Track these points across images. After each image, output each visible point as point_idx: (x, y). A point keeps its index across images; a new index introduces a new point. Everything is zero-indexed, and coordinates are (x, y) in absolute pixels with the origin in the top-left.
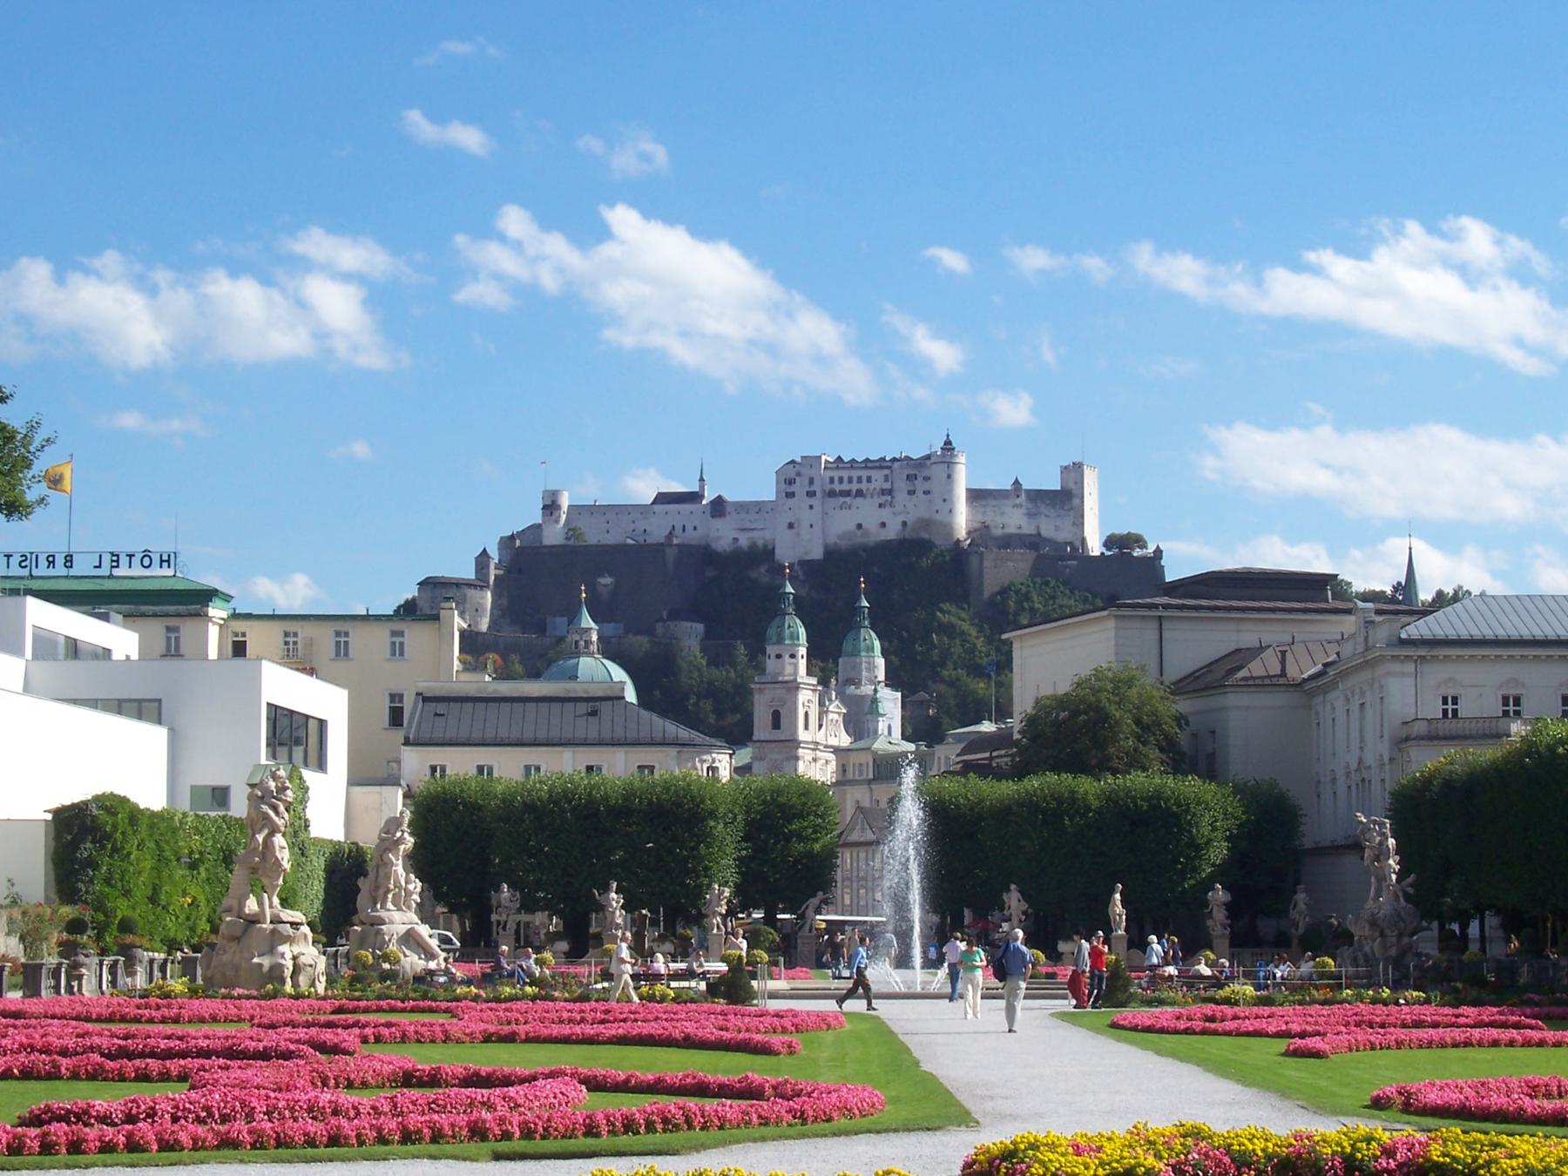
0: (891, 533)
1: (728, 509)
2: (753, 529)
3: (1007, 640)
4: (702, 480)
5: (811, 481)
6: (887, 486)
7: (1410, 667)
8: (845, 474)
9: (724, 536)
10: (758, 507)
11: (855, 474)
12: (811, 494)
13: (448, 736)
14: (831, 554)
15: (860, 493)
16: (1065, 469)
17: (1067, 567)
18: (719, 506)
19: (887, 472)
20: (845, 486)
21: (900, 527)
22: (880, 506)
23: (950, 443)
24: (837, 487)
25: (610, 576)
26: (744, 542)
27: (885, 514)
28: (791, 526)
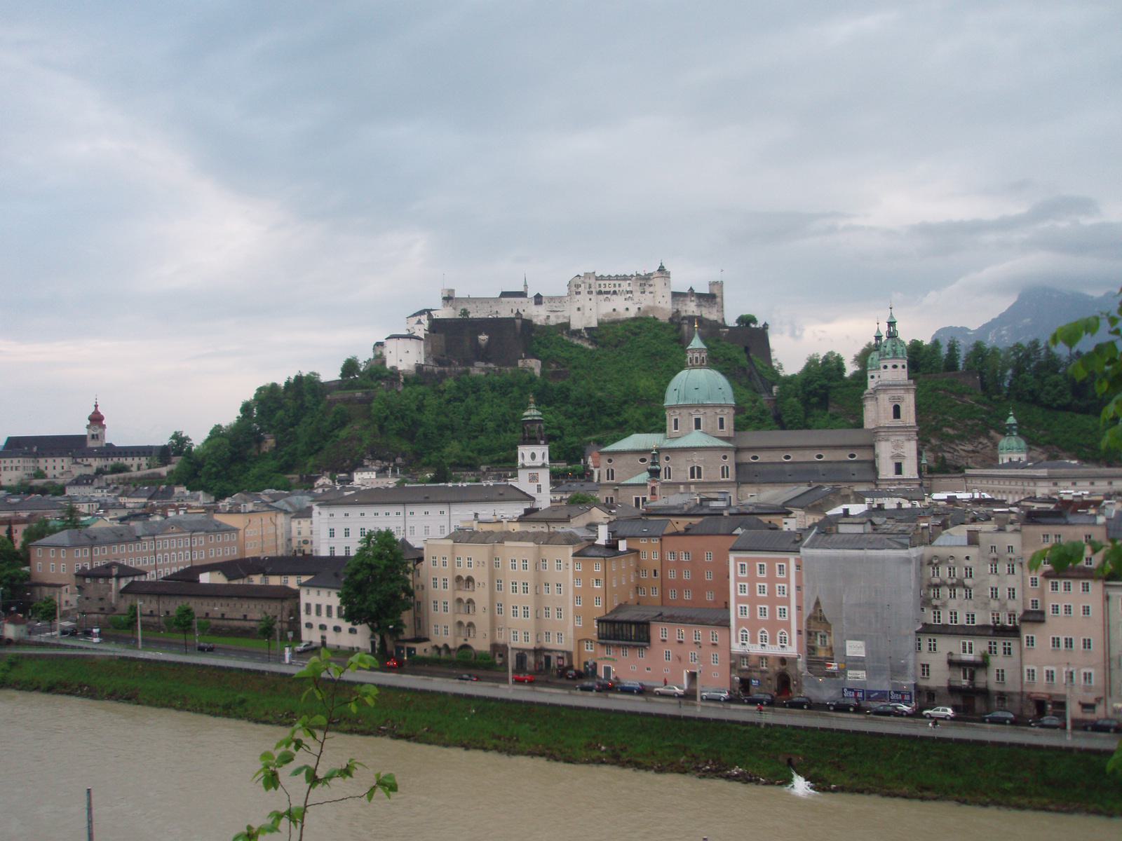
0: (632, 313)
1: (544, 301)
2: (557, 311)
4: (526, 286)
5: (590, 287)
8: (607, 282)
9: (539, 315)
10: (560, 299)
11: (612, 282)
12: (590, 293)
14: (601, 323)
15: (615, 292)
17: (724, 332)
18: (538, 299)
19: (628, 282)
20: (607, 289)
21: (637, 310)
22: (625, 299)
23: (663, 267)
24: (603, 289)
25: (486, 334)
26: (553, 321)
27: (629, 304)
28: (579, 309)
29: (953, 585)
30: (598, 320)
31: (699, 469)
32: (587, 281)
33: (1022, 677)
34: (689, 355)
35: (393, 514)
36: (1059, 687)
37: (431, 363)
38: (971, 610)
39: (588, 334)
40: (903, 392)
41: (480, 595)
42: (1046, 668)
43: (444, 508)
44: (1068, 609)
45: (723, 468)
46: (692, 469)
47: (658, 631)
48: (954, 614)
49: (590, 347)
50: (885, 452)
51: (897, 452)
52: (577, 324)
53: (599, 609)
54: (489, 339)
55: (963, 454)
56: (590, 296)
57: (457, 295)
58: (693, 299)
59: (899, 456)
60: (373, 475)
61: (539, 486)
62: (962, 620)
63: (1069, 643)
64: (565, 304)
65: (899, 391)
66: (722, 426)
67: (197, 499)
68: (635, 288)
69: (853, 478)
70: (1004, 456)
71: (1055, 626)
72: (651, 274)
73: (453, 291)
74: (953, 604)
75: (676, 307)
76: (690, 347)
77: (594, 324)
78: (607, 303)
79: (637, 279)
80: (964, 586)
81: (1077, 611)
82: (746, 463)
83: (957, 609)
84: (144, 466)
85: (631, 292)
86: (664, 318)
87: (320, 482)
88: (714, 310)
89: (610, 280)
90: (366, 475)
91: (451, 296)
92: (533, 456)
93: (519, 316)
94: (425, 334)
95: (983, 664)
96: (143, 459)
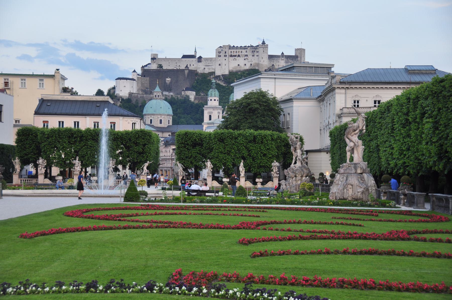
0: (247, 67)
1: (202, 60)
3: (232, 86)
4: (195, 51)
5: (225, 52)
6: (246, 54)
7: (343, 91)
8: (235, 50)
9: (201, 68)
10: (211, 59)
11: (238, 50)
12: (225, 56)
13: (49, 112)
15: (239, 56)
16: (296, 50)
19: (246, 50)
20: (235, 54)
21: (249, 65)
22: (245, 59)
23: (264, 42)
24: (233, 54)
27: (246, 62)
28: (220, 65)
37: (141, 93)
39: (223, 78)
40: (212, 110)
49: (224, 85)
56: (225, 58)
58: (283, 58)
64: (213, 62)
65: (211, 110)
68: (249, 53)
77: (227, 73)
79: (250, 49)
85: (247, 56)
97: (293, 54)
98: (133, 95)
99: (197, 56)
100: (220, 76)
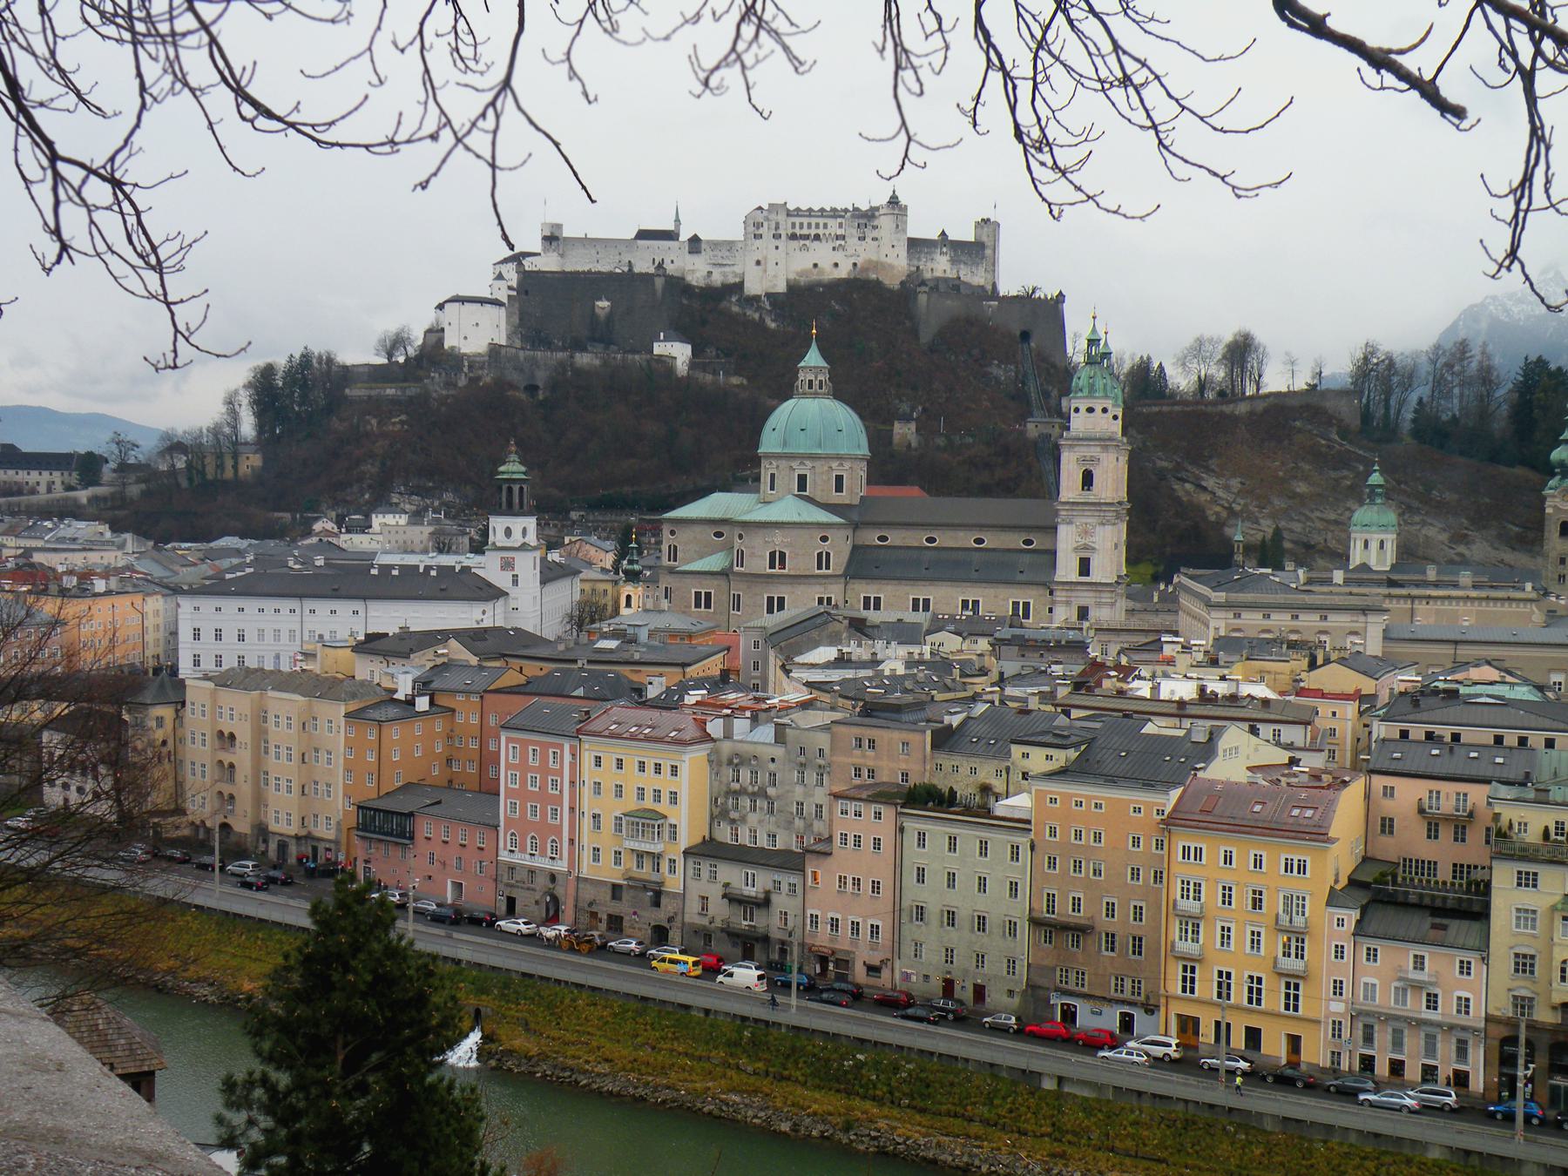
0: (843, 272)
1: (703, 246)
4: (677, 221)
5: (777, 228)
6: (840, 232)
8: (805, 221)
9: (697, 270)
10: (730, 245)
11: (814, 221)
12: (777, 236)
14: (793, 288)
15: (817, 237)
18: (695, 243)
19: (839, 220)
20: (805, 231)
21: (851, 267)
24: (798, 231)
25: (608, 300)
26: (717, 279)
27: (838, 257)
28: (758, 263)
29: (754, 794)
30: (788, 281)
31: (782, 555)
32: (773, 216)
33: (804, 924)
34: (801, 376)
35: (285, 611)
36: (844, 941)
38: (773, 829)
40: (1098, 449)
41: (242, 757)
42: (830, 915)
43: (358, 605)
44: (857, 839)
45: (820, 555)
46: (772, 555)
47: (424, 828)
48: (753, 832)
50: (1067, 540)
51: (1083, 541)
52: (753, 287)
53: (368, 791)
54: (612, 307)
55: (1319, 525)
56: (777, 242)
57: (566, 233)
58: (944, 250)
59: (1086, 548)
60: (403, 520)
61: (515, 576)
62: (763, 842)
63: (857, 882)
65: (1092, 449)
66: (839, 488)
67: (121, 546)
68: (852, 232)
69: (1020, 577)
70: (1358, 535)
71: (844, 862)
72: (877, 209)
73: (559, 226)
74: (753, 818)
75: (916, 263)
76: (802, 364)
78: (804, 253)
79: (853, 216)
80: (766, 796)
81: (867, 843)
82: (868, 546)
83: (756, 829)
84: (58, 486)
85: (843, 237)
86: (892, 281)
87: (318, 527)
88: (981, 270)
89: (810, 216)
90: (390, 519)
91: (556, 234)
92: (508, 532)
93: (661, 272)
94: (509, 296)
95: (765, 902)
96: (57, 474)
97: (969, 236)
98: (503, 351)
99: (685, 236)
100: (760, 296)
